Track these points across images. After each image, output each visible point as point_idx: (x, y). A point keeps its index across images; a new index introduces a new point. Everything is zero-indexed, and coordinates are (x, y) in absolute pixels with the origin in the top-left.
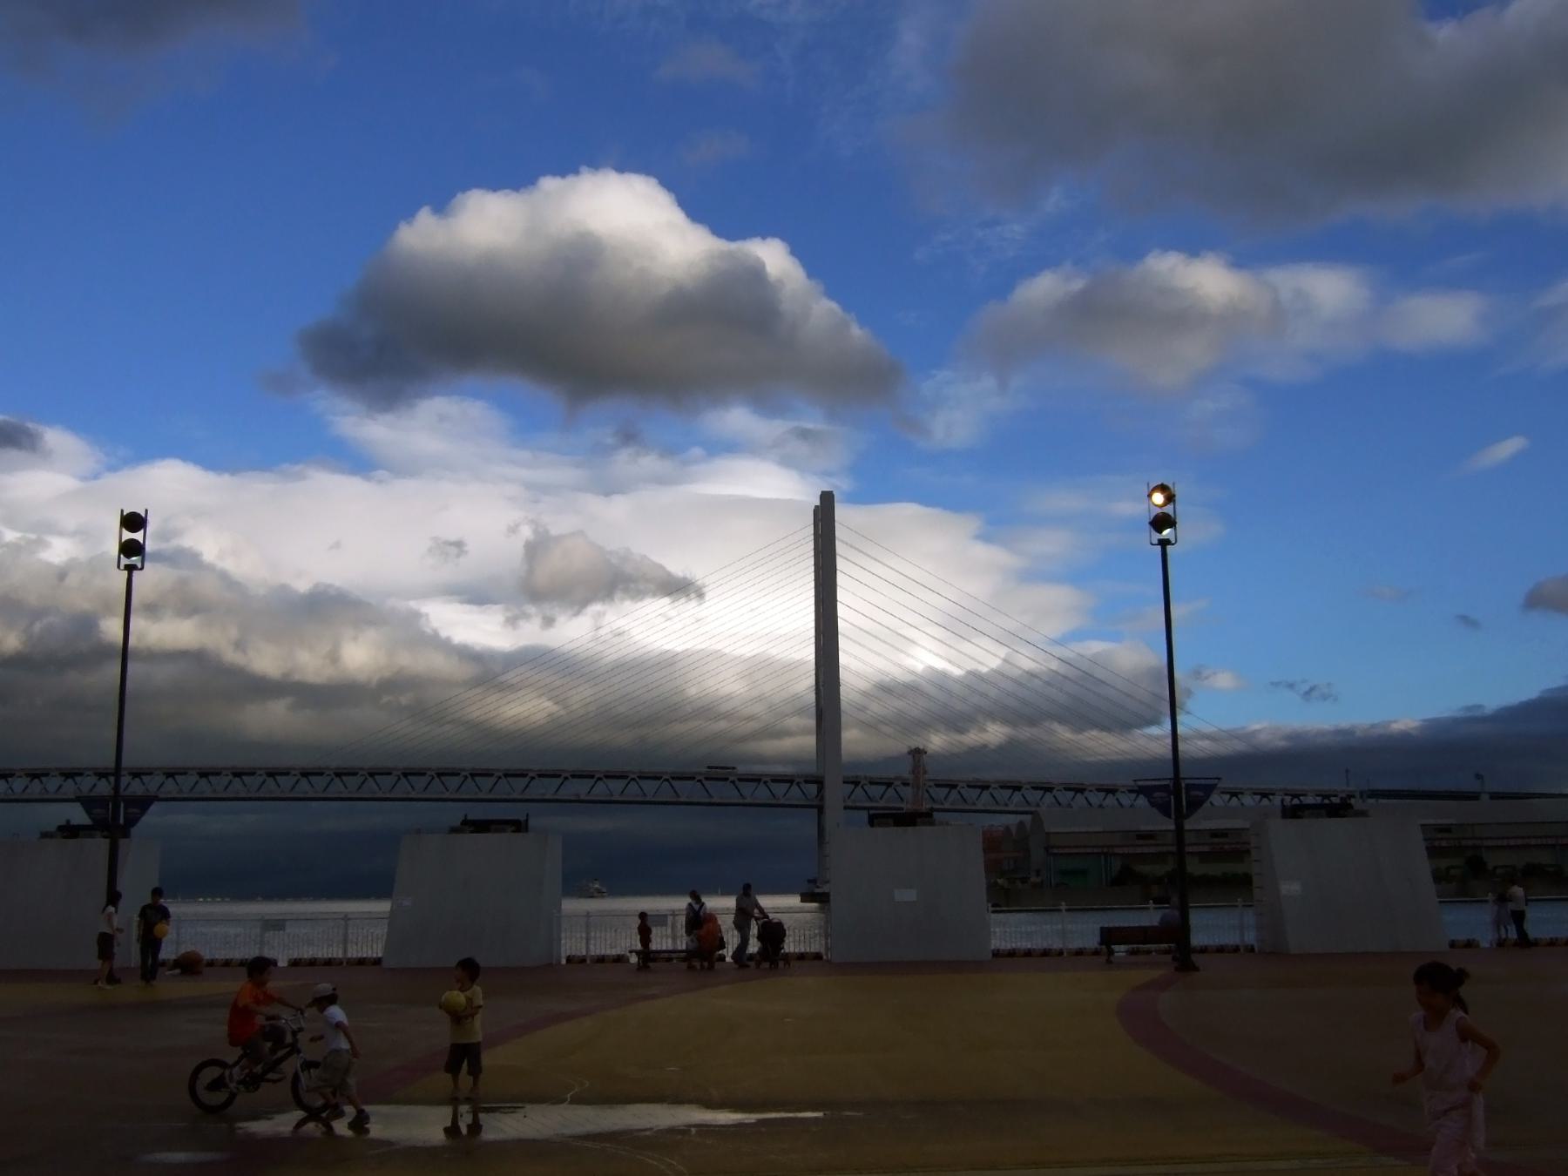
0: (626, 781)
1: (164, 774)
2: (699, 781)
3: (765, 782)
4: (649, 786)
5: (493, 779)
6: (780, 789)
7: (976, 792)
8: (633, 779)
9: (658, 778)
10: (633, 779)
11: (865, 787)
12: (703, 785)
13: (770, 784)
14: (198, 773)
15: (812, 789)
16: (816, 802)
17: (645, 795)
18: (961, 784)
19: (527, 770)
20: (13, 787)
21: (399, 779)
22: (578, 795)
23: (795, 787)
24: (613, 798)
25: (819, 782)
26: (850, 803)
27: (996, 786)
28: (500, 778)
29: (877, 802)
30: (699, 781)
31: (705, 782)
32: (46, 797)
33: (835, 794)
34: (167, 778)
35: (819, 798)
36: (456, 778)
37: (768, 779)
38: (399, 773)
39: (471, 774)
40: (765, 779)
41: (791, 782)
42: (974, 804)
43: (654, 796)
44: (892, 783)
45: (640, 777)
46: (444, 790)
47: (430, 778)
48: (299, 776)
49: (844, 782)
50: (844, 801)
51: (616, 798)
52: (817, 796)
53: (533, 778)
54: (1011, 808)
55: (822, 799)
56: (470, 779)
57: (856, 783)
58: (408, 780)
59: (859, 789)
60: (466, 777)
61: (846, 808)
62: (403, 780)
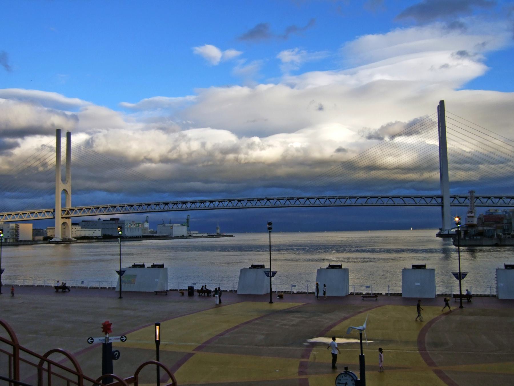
0: (367, 199)
1: (238, 201)
2: (412, 198)
3: (423, 198)
4: (385, 201)
5: (346, 199)
6: (428, 200)
7: (486, 200)
8: (380, 198)
9: (388, 198)
10: (380, 198)
11: (458, 199)
12: (414, 200)
13: (436, 199)
14: (247, 200)
15: (439, 200)
16: (441, 204)
17: (384, 204)
18: (480, 197)
19: (356, 196)
20: (187, 206)
21: (306, 200)
22: (362, 204)
23: (433, 200)
24: (384, 205)
25: (442, 197)
26: (452, 204)
27: (153, 204)
28: (337, 199)
29: (462, 204)
30: (412, 198)
31: (414, 199)
32: (224, 208)
33: (447, 201)
34: (238, 202)
35: (442, 203)
36: (313, 200)
37: (424, 197)
38: (306, 198)
39: (338, 198)
40: (434, 197)
41: (432, 198)
42: (497, 204)
43: (354, 204)
44: (467, 198)
45: (382, 198)
46: (341, 203)
47: (306, 200)
48: (286, 200)
49: (450, 198)
50: (451, 204)
51: (374, 204)
52: (441, 202)
53: (347, 199)
54: (510, 205)
55: (443, 203)
56: (328, 200)
57: (455, 198)
58: (329, 200)
59: (456, 200)
60: (327, 199)
61: (451, 206)
62: (307, 200)
